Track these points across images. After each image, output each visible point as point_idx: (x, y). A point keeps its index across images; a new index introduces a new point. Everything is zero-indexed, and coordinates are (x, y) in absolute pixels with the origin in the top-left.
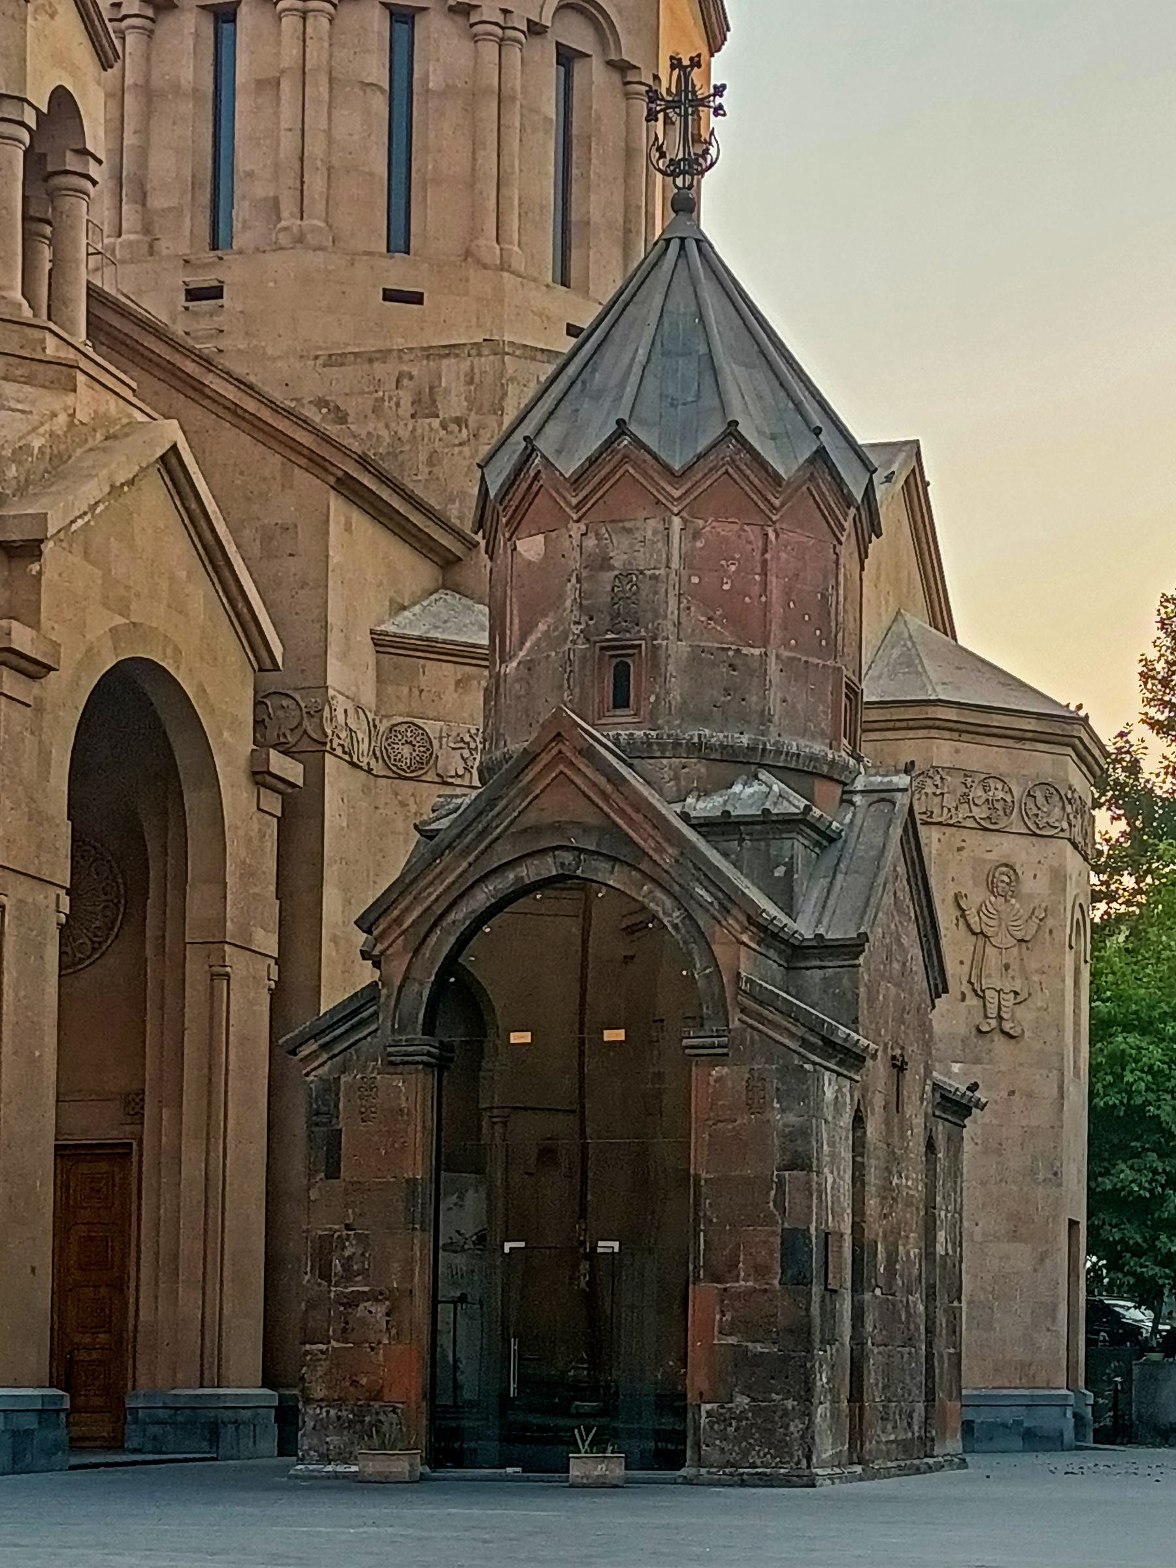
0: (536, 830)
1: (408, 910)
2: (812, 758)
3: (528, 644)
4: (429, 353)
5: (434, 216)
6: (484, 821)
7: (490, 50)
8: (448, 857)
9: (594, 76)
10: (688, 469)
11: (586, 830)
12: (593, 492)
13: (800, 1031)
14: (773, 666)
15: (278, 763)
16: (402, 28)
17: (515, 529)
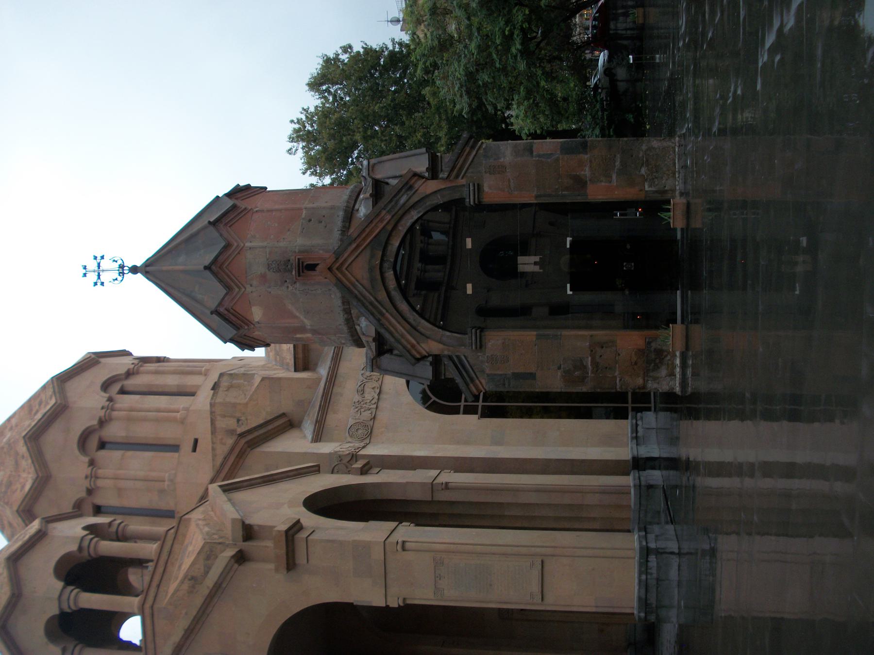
0: (372, 280)
1: (408, 341)
2: (352, 192)
3: (298, 314)
4: (214, 432)
5: (168, 433)
6: (367, 304)
7: (115, 414)
8: (384, 321)
9: (131, 383)
10: (225, 239)
11: (372, 256)
12: (233, 281)
13: (468, 149)
14: (311, 205)
15: (358, 465)
16: (107, 446)
17: (248, 322)
